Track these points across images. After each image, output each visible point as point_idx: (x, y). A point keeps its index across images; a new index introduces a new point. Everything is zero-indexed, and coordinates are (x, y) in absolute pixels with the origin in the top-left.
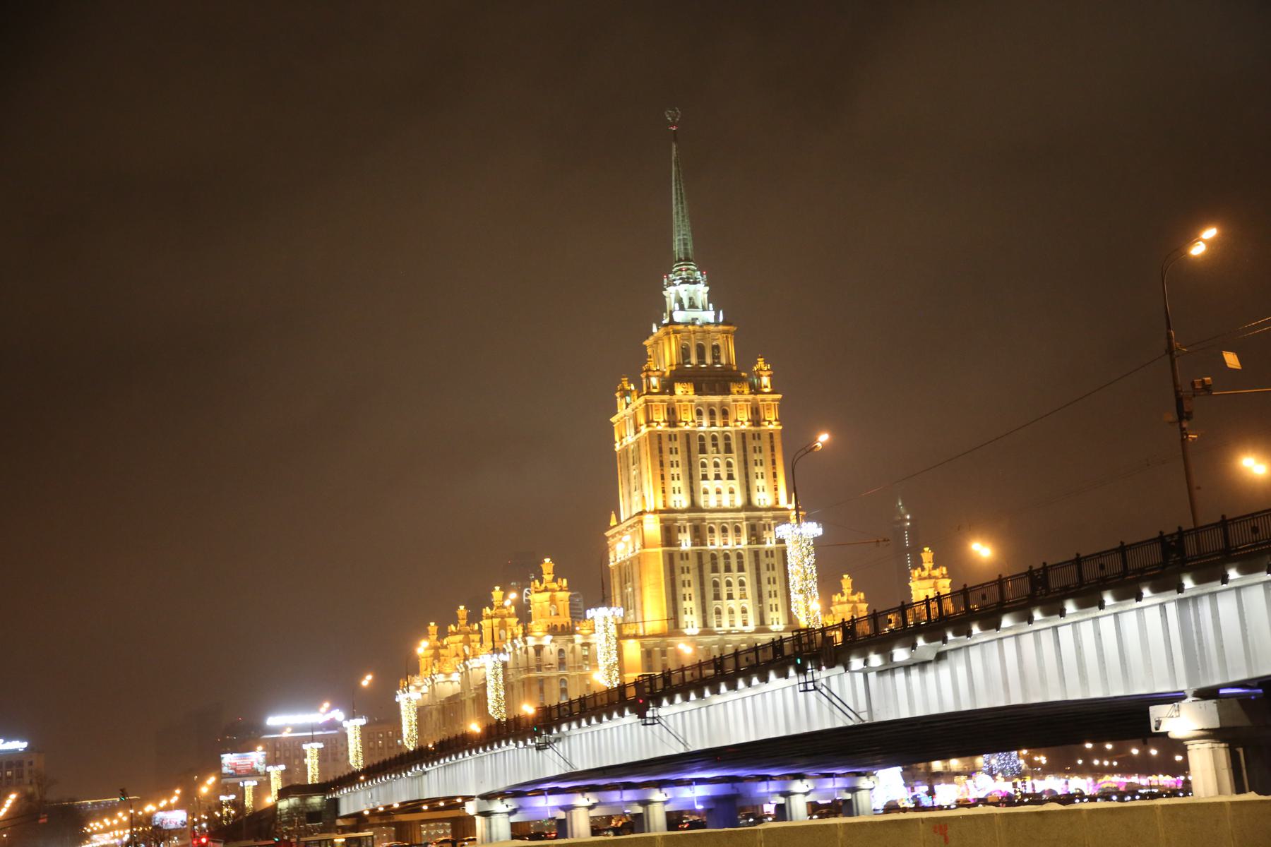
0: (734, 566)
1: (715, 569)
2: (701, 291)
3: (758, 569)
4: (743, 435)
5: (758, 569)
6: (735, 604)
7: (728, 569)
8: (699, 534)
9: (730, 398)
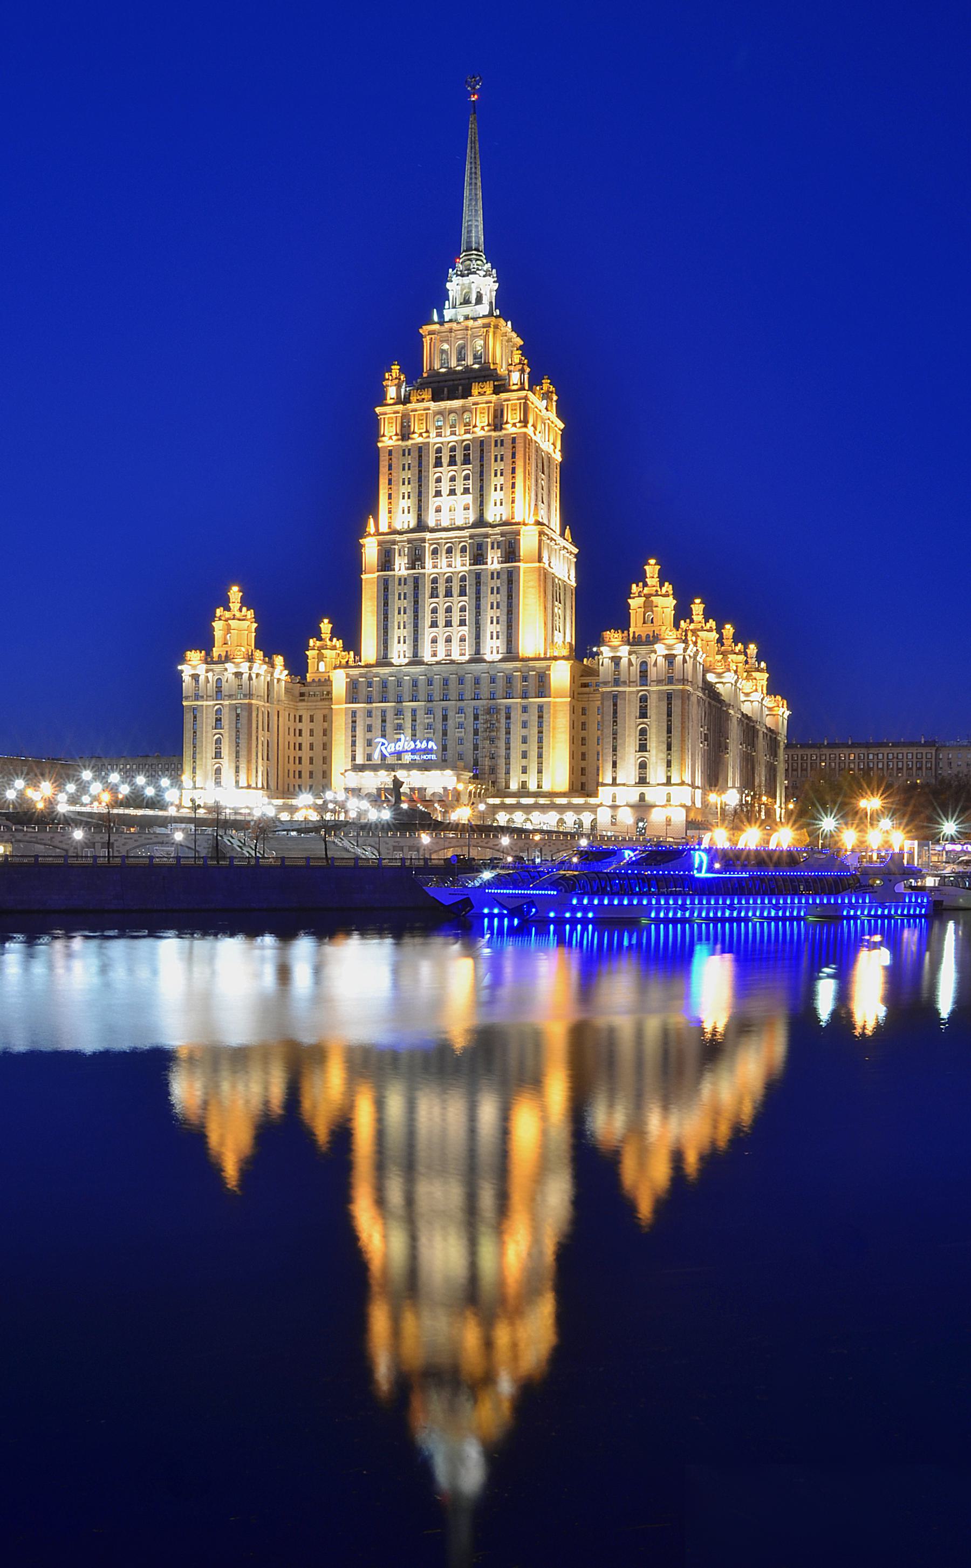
0: (456, 591)
3: (478, 592)
4: (482, 443)
5: (478, 592)
6: (458, 632)
7: (449, 594)
8: (416, 559)
9: (471, 400)
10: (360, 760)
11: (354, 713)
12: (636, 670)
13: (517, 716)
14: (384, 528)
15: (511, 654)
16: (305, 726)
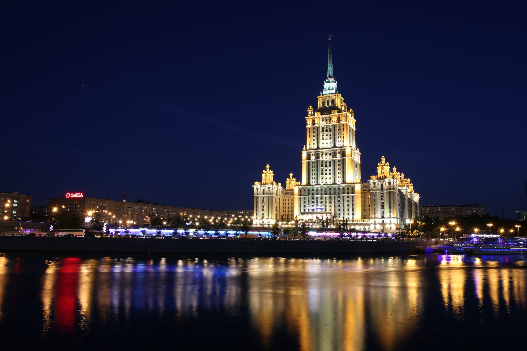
0: (328, 165)
1: (322, 166)
2: (334, 85)
3: (334, 165)
5: (334, 165)
6: (328, 176)
7: (326, 166)
10: (302, 211)
11: (300, 198)
12: (380, 186)
13: (346, 199)
14: (308, 148)
15: (344, 182)
16: (287, 202)
